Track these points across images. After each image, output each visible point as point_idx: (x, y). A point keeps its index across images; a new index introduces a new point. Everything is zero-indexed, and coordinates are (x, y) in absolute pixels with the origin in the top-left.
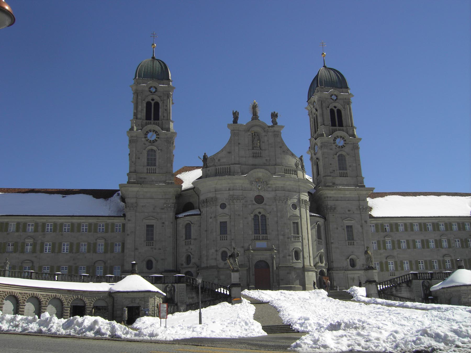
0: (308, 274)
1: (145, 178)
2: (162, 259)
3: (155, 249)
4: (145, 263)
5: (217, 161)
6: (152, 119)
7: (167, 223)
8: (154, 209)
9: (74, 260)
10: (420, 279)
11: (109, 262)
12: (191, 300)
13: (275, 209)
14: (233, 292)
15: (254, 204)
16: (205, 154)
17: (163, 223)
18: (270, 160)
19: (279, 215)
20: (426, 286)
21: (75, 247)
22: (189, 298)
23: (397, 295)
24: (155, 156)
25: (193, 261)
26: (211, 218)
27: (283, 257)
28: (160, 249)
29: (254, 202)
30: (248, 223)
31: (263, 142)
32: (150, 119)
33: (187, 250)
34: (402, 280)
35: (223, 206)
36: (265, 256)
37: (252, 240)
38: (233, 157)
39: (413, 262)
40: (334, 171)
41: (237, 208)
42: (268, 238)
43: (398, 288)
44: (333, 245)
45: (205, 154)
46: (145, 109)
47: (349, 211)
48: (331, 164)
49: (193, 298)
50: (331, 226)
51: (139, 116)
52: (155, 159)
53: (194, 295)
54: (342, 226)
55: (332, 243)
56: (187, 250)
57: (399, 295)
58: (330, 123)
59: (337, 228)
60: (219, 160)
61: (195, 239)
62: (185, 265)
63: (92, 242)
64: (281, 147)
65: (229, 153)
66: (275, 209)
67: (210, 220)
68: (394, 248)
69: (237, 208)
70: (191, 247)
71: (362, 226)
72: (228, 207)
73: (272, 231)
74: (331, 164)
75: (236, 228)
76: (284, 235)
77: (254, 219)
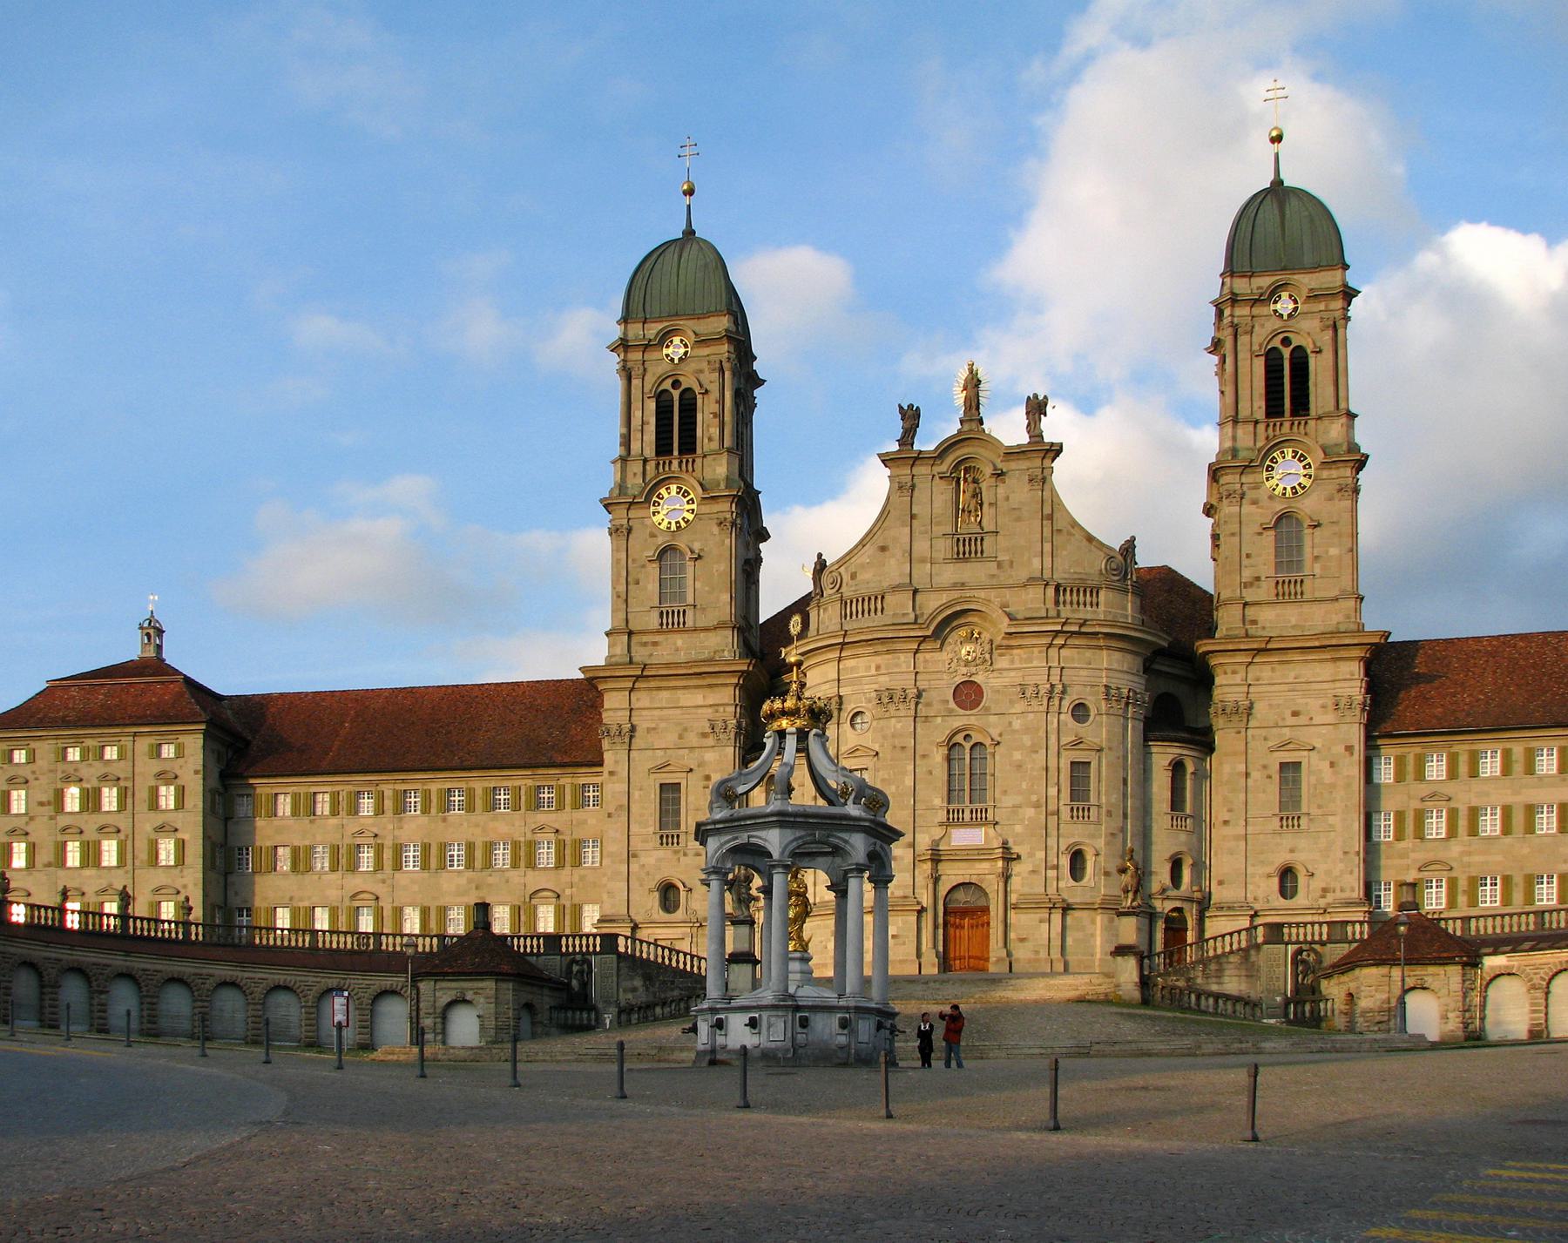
1: (655, 644)
6: (676, 453)
12: (630, 996)
13: (1017, 724)
15: (950, 713)
16: (820, 555)
20: (1303, 961)
23: (1206, 988)
24: (682, 568)
29: (952, 705)
32: (671, 452)
36: (986, 872)
37: (941, 824)
39: (1518, 880)
40: (1258, 579)
43: (1213, 967)
45: (820, 555)
46: (653, 420)
48: (1248, 556)
49: (634, 990)
51: (635, 447)
53: (638, 982)
57: (1215, 988)
60: (853, 576)
65: (883, 549)
69: (899, 726)
71: (1332, 765)
74: (1248, 556)
77: (949, 759)
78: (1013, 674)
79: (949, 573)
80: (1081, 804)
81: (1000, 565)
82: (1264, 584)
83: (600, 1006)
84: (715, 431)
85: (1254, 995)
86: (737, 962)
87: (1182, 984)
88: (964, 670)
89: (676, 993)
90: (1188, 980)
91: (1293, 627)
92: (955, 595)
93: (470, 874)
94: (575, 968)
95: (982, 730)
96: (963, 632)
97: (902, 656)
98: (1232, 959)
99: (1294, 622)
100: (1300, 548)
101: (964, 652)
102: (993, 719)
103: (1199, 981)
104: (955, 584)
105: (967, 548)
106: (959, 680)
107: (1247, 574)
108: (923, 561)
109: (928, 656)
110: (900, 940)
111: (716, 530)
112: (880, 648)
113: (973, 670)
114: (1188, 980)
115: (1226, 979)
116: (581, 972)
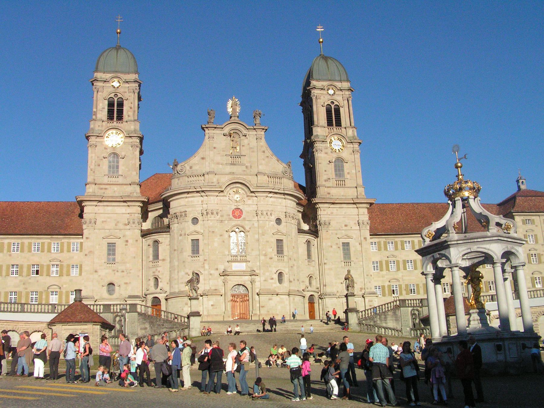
0: (294, 299)
2: (126, 283)
3: (117, 271)
4: (105, 288)
5: (188, 168)
6: (115, 119)
7: (130, 241)
8: (116, 225)
9: (24, 284)
10: (408, 307)
11: (64, 286)
12: (143, 331)
13: (256, 225)
14: (191, 323)
15: (230, 219)
17: (127, 241)
18: (251, 167)
19: (260, 232)
20: (415, 314)
21: (25, 270)
22: (141, 329)
23: (381, 325)
25: (160, 285)
26: (181, 235)
27: (265, 280)
28: (123, 272)
29: (231, 216)
30: (224, 242)
31: (243, 146)
33: (154, 272)
34: (388, 308)
35: (195, 221)
38: (207, 163)
40: (329, 179)
41: (211, 224)
42: (248, 258)
43: (383, 316)
44: (326, 267)
46: (106, 108)
47: (346, 226)
48: (325, 171)
49: (146, 328)
50: (324, 244)
52: (118, 167)
53: (147, 325)
54: (337, 244)
55: (325, 264)
56: (154, 272)
57: (384, 325)
58: (326, 122)
59: (331, 246)
60: (191, 168)
61: (164, 260)
62: (152, 289)
63: (45, 264)
64: (264, 152)
65: (203, 158)
66: (256, 225)
67: (180, 238)
68: (398, 269)
69: (211, 224)
70: (159, 269)
72: (200, 222)
73: (252, 250)
75: (210, 247)
76: (265, 255)
78: (254, 206)
79: (229, 169)
80: (280, 255)
81: (247, 167)
82: (331, 180)
83: (130, 336)
84: (131, 113)
85: (399, 328)
86: (193, 316)
87: (372, 323)
88: (236, 204)
89: (165, 330)
90: (375, 322)
91: (343, 196)
92: (231, 176)
93: (21, 278)
94: (118, 319)
95: (243, 227)
96: (235, 190)
97: (212, 198)
98: (390, 313)
99: (342, 194)
100: (343, 170)
101: (235, 198)
102: (247, 222)
103: (378, 322)
104: (230, 173)
105: (236, 158)
106: (234, 207)
107: (325, 177)
108: (218, 164)
109: (222, 198)
110: (215, 307)
111: (131, 149)
112: (203, 194)
113: (239, 204)
114: (375, 322)
115: (388, 321)
116: (121, 321)
